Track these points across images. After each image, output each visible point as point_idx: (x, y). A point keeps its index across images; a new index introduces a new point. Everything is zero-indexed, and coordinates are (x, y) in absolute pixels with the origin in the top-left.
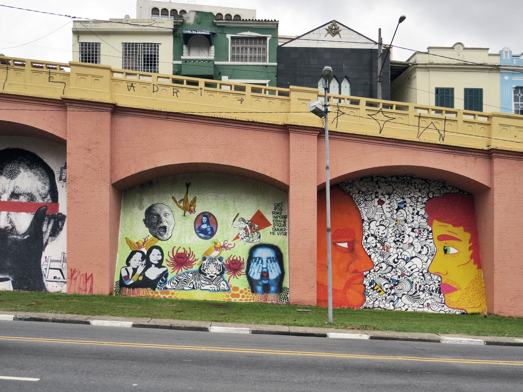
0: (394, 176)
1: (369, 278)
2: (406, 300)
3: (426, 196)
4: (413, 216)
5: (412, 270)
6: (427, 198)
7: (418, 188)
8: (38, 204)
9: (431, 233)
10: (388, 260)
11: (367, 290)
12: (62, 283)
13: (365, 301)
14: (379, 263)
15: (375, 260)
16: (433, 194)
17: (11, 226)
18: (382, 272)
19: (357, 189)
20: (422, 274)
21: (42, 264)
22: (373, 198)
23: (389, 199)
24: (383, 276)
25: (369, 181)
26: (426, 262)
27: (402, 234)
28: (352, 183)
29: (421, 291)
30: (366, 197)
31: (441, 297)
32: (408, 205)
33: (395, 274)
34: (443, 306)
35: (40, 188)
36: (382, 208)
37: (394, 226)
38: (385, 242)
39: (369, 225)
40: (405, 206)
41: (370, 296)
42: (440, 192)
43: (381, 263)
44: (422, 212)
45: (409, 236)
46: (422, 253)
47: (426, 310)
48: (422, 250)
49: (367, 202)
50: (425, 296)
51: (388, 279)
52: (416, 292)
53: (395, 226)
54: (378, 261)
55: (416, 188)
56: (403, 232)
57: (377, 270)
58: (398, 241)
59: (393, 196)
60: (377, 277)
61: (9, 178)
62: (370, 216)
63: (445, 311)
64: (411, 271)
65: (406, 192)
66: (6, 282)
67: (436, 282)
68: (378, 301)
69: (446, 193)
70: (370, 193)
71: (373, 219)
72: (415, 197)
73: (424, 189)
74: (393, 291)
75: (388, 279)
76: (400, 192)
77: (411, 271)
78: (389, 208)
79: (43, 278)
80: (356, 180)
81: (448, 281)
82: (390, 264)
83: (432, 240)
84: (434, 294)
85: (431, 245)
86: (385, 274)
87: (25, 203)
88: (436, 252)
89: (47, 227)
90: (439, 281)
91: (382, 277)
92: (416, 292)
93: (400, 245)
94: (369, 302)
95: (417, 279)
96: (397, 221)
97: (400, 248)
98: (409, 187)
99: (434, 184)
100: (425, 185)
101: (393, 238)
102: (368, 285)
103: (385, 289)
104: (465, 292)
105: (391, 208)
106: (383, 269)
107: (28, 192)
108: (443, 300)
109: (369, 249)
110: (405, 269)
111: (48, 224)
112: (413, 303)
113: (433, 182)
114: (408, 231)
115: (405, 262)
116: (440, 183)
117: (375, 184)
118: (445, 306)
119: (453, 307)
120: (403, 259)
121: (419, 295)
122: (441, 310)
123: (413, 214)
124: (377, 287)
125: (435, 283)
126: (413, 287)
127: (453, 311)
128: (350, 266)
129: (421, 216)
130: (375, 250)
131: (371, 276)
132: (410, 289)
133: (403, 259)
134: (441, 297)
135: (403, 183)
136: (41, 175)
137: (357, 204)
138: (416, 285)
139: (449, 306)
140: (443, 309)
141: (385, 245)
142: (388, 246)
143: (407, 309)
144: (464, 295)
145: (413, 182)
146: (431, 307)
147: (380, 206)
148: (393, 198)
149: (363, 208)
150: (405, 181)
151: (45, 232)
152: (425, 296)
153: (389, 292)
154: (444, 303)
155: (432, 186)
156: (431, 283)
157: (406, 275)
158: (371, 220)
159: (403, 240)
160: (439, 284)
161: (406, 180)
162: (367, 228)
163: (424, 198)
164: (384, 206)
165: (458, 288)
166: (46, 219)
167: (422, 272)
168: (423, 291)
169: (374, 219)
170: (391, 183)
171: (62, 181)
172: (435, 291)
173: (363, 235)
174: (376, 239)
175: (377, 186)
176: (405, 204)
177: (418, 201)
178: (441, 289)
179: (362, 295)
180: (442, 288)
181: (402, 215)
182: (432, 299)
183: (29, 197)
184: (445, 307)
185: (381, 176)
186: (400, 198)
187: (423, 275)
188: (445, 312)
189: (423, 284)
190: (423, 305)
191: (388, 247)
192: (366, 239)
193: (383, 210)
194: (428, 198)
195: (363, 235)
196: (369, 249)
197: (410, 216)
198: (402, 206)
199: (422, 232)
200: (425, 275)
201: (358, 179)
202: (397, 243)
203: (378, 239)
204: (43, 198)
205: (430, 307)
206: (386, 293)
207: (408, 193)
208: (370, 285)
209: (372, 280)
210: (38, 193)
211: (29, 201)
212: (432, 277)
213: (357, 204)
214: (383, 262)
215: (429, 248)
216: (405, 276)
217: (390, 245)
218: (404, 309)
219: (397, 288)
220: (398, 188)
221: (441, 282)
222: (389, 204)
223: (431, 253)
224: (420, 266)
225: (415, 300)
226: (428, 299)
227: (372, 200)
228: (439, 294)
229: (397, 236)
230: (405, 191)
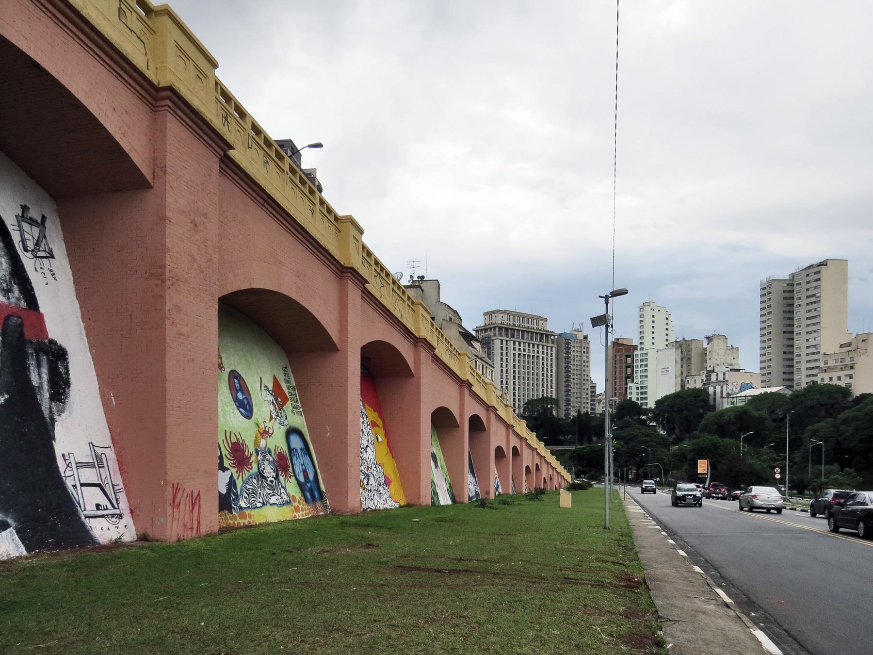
12: (114, 519)
21: (63, 475)
89: (40, 377)
111: (39, 366)
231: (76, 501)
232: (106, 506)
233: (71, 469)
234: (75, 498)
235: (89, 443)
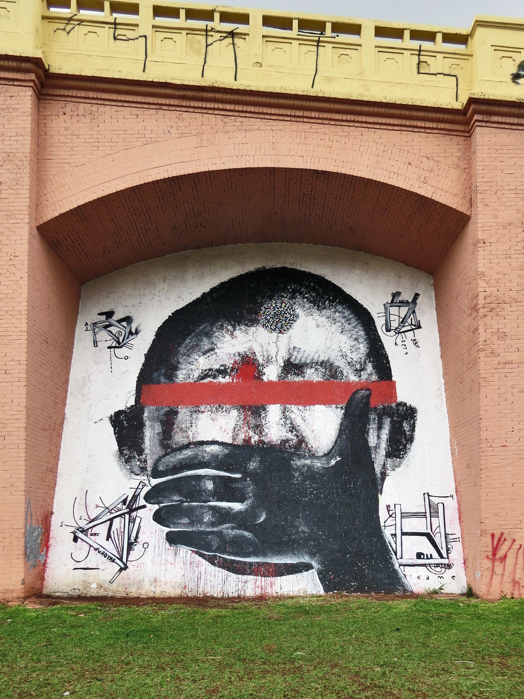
8: (348, 384)
17: (295, 438)
21: (382, 524)
35: (346, 349)
61: (275, 329)
66: (305, 573)
79: (391, 558)
87: (319, 382)
89: (379, 437)
107: (321, 359)
111: (380, 428)
136: (344, 322)
151: (376, 447)
166: (372, 417)
171: (392, 333)
183: (326, 369)
204: (358, 372)
210: (344, 360)
211: (327, 379)
231: (393, 549)
232: (431, 555)
233: (395, 519)
234: (391, 546)
235: (424, 494)
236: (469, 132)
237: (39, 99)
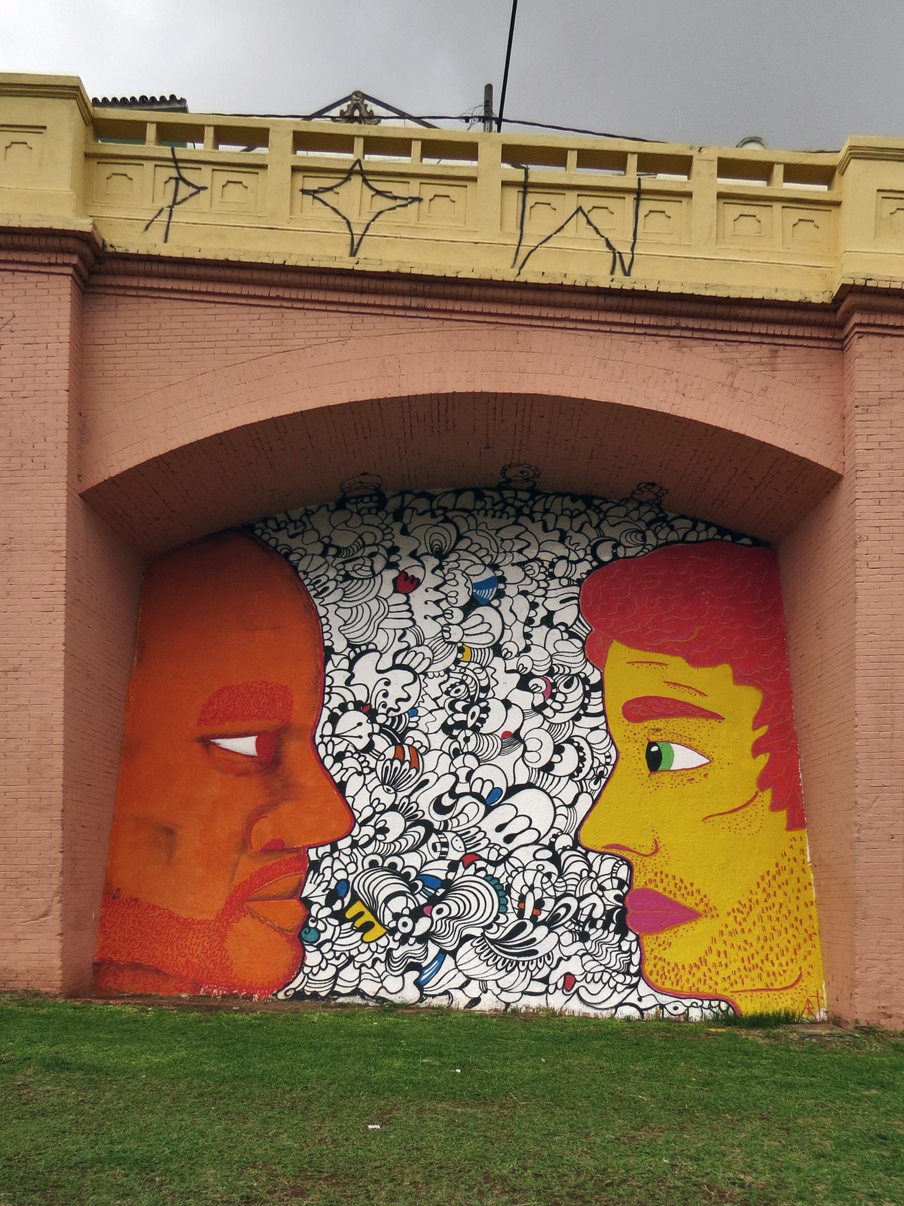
0: (465, 490)
1: (328, 872)
2: (477, 961)
3: (586, 555)
4: (527, 629)
5: (509, 839)
6: (590, 563)
7: (555, 529)
9: (599, 694)
10: (413, 799)
11: (316, 920)
13: (301, 969)
14: (375, 813)
15: (361, 802)
16: (615, 547)
18: (382, 848)
19: (320, 541)
20: (548, 854)
22: (378, 567)
23: (438, 572)
24: (386, 865)
25: (369, 509)
26: (568, 806)
27: (480, 700)
28: (305, 519)
29: (543, 923)
30: (349, 567)
31: (625, 946)
32: (511, 590)
33: (436, 855)
34: (635, 986)
36: (407, 603)
37: (447, 671)
38: (408, 729)
39: (350, 669)
40: (500, 594)
41: (326, 948)
42: (644, 538)
43: (382, 813)
44: (567, 615)
45: (507, 704)
46: (558, 770)
47: (557, 1001)
48: (556, 758)
49: (354, 585)
50: (559, 942)
51: (405, 877)
52: (521, 928)
53: (452, 667)
54: (371, 805)
55: (550, 526)
56: (485, 689)
57: (366, 839)
58: (462, 725)
59: (456, 561)
60: (360, 869)
62: (356, 634)
63: (642, 1005)
64: (503, 844)
65: (507, 545)
67: (608, 885)
68: (357, 965)
69: (668, 543)
70: (368, 550)
71: (367, 645)
72: (542, 561)
73: (580, 531)
74: (423, 925)
75: (405, 877)
76: (485, 543)
77: (503, 844)
78: (437, 603)
80: (320, 507)
81: (658, 879)
82: (420, 814)
83: (602, 719)
84: (594, 934)
85: (597, 737)
86: (398, 855)
88: (614, 765)
90: (620, 880)
91: (383, 869)
92: (521, 928)
93: (467, 739)
94: (315, 970)
95: (529, 876)
96: (461, 650)
97: (466, 754)
98: (521, 525)
99: (621, 511)
100: (583, 518)
101: (441, 716)
102: (322, 900)
103: (388, 917)
104: (733, 926)
105: (444, 605)
106: (391, 837)
108: (636, 959)
109: (339, 757)
110: (481, 835)
112: (503, 972)
113: (618, 505)
114: (506, 685)
115: (482, 807)
116: (644, 509)
117: (389, 520)
118: (642, 985)
119: (678, 988)
120: (478, 796)
121: (534, 940)
122: (621, 1004)
123: (529, 621)
124: (358, 907)
125: (601, 888)
126: (509, 906)
127: (674, 1007)
128: (256, 827)
129: (563, 628)
130: (365, 764)
131: (337, 866)
132: (497, 917)
133: (478, 796)
134: (625, 946)
135: (498, 514)
137: (313, 593)
138: (522, 898)
139: (659, 984)
140: (633, 999)
141: (409, 741)
142: (417, 745)
143: (476, 1001)
144: (726, 937)
145: (539, 507)
146: (582, 992)
147: (402, 598)
148: (455, 565)
149: (332, 608)
150: (507, 505)
152: (559, 942)
153: (406, 930)
154: (639, 974)
155: (613, 520)
156: (587, 890)
157: (482, 859)
158: (357, 651)
159: (482, 721)
160: (618, 892)
161: (510, 501)
162: (340, 678)
163: (576, 562)
164: (418, 597)
165: (701, 908)
167: (551, 847)
168: (552, 923)
169: (371, 647)
170: (450, 515)
172: (600, 924)
173: (323, 705)
174: (372, 720)
175: (397, 526)
176: (501, 586)
177: (552, 576)
178: (628, 916)
179: (290, 941)
180: (630, 911)
181: (485, 627)
182: (587, 958)
184: (643, 988)
185: (417, 491)
186: (483, 567)
187: (555, 859)
188: (641, 1011)
189: (552, 893)
190: (545, 980)
191: (417, 750)
192: (334, 719)
193: (410, 610)
194: (595, 564)
195: (323, 705)
196: (339, 757)
197: (518, 629)
198: (488, 594)
199: (562, 688)
200: (563, 857)
201: (328, 506)
202: (455, 732)
203: (381, 719)
205: (577, 991)
206: (393, 931)
207: (516, 548)
208: (329, 902)
209: (339, 882)
212: (590, 866)
213: (313, 593)
214: (394, 808)
215: (587, 750)
216: (480, 864)
217: (426, 744)
218: (461, 1000)
219: (440, 911)
220: (476, 530)
221: (630, 886)
222: (437, 589)
223: (592, 768)
224: (542, 823)
225: (511, 962)
226: (569, 958)
227: (374, 575)
228: (618, 937)
229: (459, 706)
230: (503, 540)
236: (841, 341)
237: (84, 292)
